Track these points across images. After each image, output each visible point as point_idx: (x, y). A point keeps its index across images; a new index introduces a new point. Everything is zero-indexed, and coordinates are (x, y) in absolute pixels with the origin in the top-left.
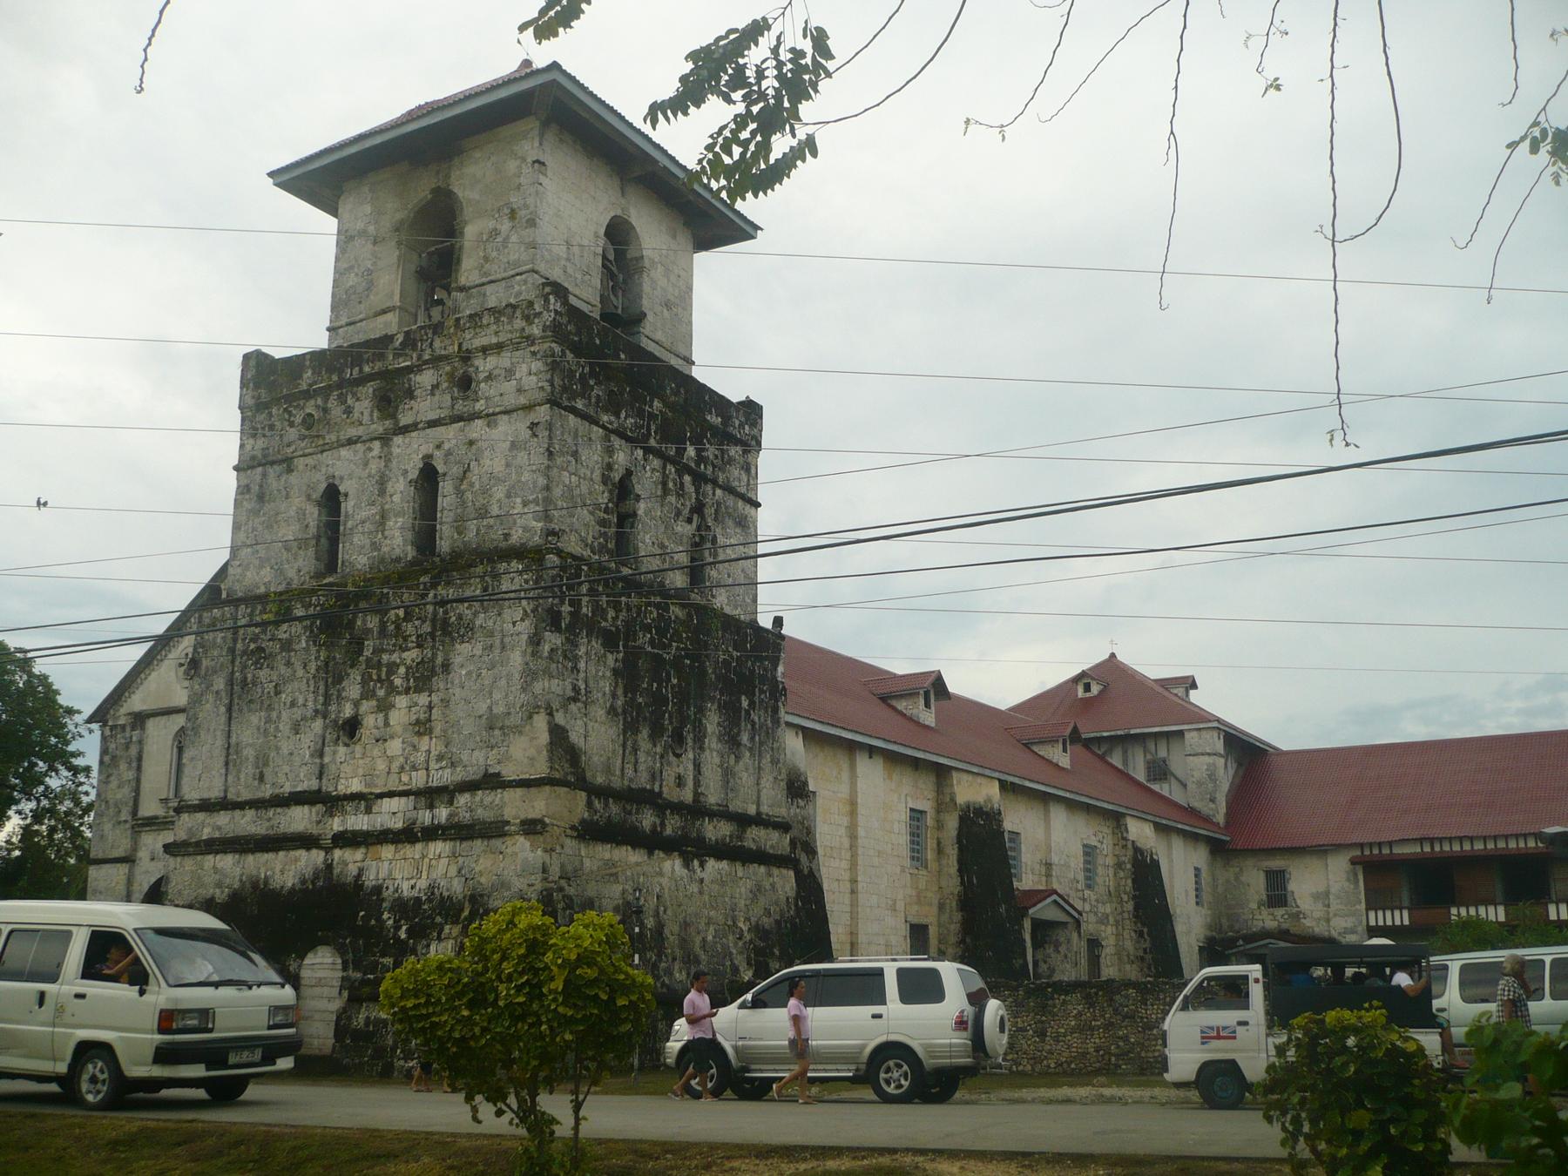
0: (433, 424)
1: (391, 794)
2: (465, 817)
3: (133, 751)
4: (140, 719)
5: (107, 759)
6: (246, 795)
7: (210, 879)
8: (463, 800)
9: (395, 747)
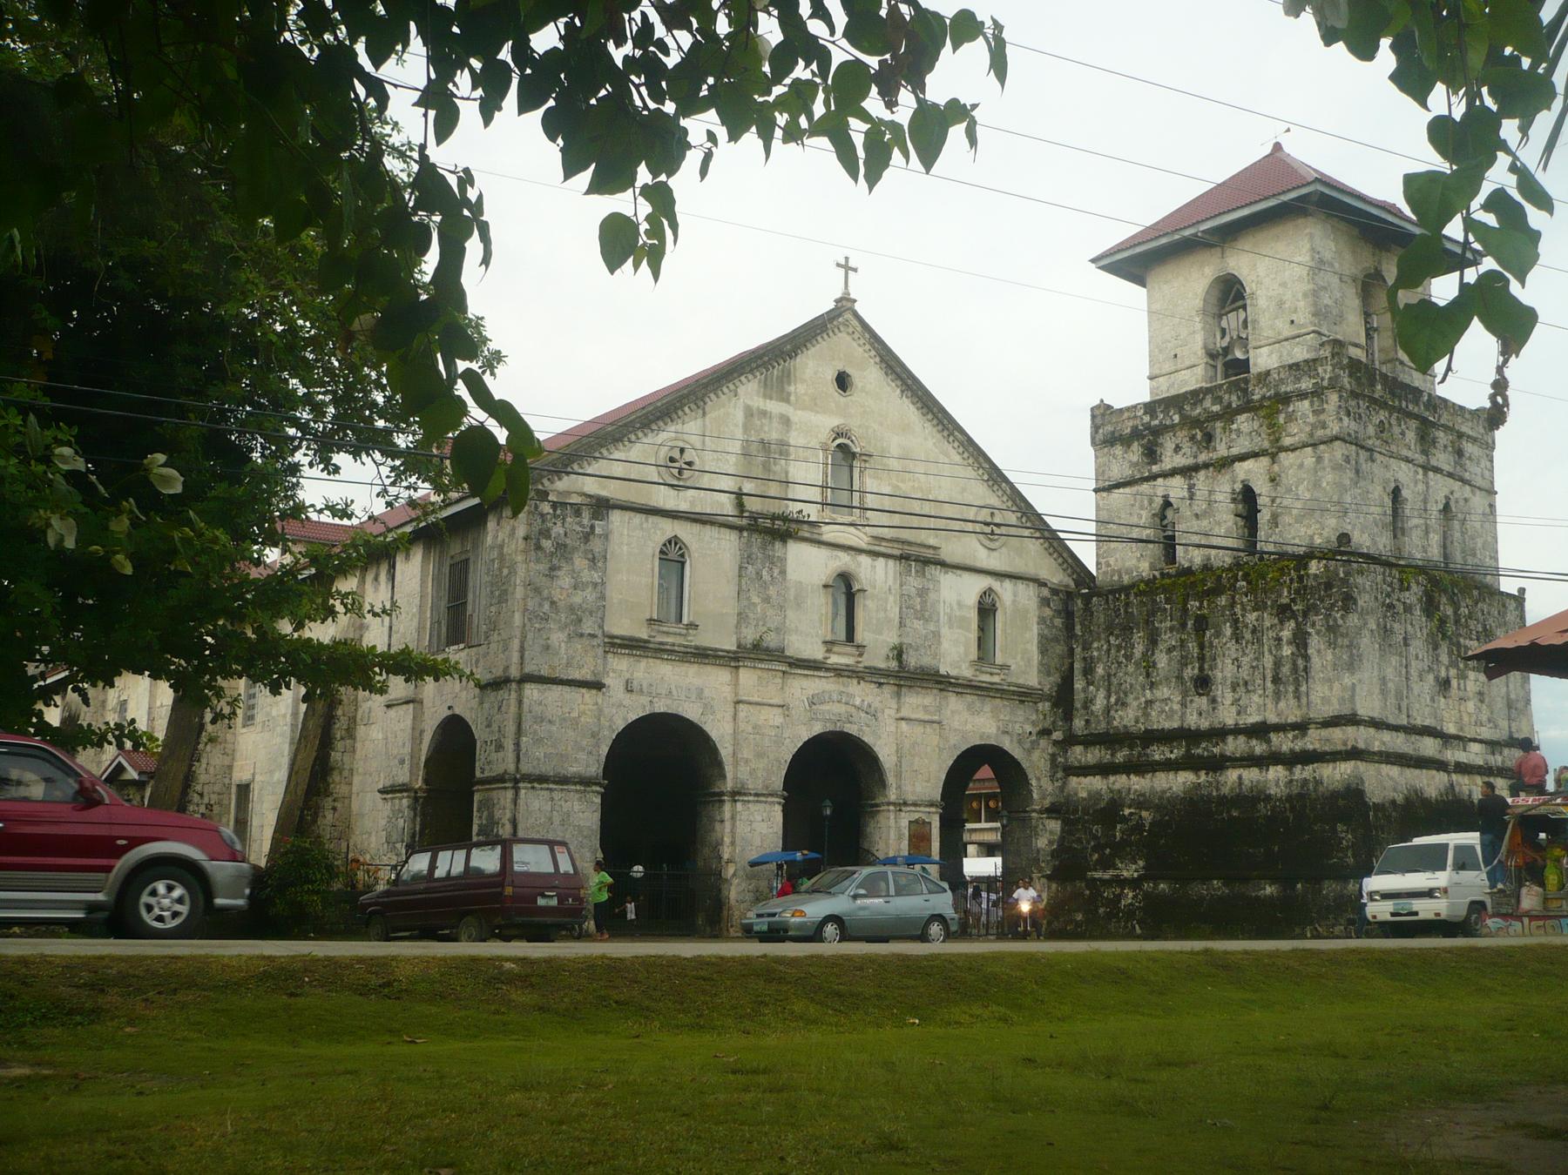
0: (1450, 475)
1: (1475, 740)
3: (596, 545)
4: (601, 506)
5: (546, 544)
6: (1392, 721)
7: (1389, 784)
8: (1506, 751)
9: (1471, 706)
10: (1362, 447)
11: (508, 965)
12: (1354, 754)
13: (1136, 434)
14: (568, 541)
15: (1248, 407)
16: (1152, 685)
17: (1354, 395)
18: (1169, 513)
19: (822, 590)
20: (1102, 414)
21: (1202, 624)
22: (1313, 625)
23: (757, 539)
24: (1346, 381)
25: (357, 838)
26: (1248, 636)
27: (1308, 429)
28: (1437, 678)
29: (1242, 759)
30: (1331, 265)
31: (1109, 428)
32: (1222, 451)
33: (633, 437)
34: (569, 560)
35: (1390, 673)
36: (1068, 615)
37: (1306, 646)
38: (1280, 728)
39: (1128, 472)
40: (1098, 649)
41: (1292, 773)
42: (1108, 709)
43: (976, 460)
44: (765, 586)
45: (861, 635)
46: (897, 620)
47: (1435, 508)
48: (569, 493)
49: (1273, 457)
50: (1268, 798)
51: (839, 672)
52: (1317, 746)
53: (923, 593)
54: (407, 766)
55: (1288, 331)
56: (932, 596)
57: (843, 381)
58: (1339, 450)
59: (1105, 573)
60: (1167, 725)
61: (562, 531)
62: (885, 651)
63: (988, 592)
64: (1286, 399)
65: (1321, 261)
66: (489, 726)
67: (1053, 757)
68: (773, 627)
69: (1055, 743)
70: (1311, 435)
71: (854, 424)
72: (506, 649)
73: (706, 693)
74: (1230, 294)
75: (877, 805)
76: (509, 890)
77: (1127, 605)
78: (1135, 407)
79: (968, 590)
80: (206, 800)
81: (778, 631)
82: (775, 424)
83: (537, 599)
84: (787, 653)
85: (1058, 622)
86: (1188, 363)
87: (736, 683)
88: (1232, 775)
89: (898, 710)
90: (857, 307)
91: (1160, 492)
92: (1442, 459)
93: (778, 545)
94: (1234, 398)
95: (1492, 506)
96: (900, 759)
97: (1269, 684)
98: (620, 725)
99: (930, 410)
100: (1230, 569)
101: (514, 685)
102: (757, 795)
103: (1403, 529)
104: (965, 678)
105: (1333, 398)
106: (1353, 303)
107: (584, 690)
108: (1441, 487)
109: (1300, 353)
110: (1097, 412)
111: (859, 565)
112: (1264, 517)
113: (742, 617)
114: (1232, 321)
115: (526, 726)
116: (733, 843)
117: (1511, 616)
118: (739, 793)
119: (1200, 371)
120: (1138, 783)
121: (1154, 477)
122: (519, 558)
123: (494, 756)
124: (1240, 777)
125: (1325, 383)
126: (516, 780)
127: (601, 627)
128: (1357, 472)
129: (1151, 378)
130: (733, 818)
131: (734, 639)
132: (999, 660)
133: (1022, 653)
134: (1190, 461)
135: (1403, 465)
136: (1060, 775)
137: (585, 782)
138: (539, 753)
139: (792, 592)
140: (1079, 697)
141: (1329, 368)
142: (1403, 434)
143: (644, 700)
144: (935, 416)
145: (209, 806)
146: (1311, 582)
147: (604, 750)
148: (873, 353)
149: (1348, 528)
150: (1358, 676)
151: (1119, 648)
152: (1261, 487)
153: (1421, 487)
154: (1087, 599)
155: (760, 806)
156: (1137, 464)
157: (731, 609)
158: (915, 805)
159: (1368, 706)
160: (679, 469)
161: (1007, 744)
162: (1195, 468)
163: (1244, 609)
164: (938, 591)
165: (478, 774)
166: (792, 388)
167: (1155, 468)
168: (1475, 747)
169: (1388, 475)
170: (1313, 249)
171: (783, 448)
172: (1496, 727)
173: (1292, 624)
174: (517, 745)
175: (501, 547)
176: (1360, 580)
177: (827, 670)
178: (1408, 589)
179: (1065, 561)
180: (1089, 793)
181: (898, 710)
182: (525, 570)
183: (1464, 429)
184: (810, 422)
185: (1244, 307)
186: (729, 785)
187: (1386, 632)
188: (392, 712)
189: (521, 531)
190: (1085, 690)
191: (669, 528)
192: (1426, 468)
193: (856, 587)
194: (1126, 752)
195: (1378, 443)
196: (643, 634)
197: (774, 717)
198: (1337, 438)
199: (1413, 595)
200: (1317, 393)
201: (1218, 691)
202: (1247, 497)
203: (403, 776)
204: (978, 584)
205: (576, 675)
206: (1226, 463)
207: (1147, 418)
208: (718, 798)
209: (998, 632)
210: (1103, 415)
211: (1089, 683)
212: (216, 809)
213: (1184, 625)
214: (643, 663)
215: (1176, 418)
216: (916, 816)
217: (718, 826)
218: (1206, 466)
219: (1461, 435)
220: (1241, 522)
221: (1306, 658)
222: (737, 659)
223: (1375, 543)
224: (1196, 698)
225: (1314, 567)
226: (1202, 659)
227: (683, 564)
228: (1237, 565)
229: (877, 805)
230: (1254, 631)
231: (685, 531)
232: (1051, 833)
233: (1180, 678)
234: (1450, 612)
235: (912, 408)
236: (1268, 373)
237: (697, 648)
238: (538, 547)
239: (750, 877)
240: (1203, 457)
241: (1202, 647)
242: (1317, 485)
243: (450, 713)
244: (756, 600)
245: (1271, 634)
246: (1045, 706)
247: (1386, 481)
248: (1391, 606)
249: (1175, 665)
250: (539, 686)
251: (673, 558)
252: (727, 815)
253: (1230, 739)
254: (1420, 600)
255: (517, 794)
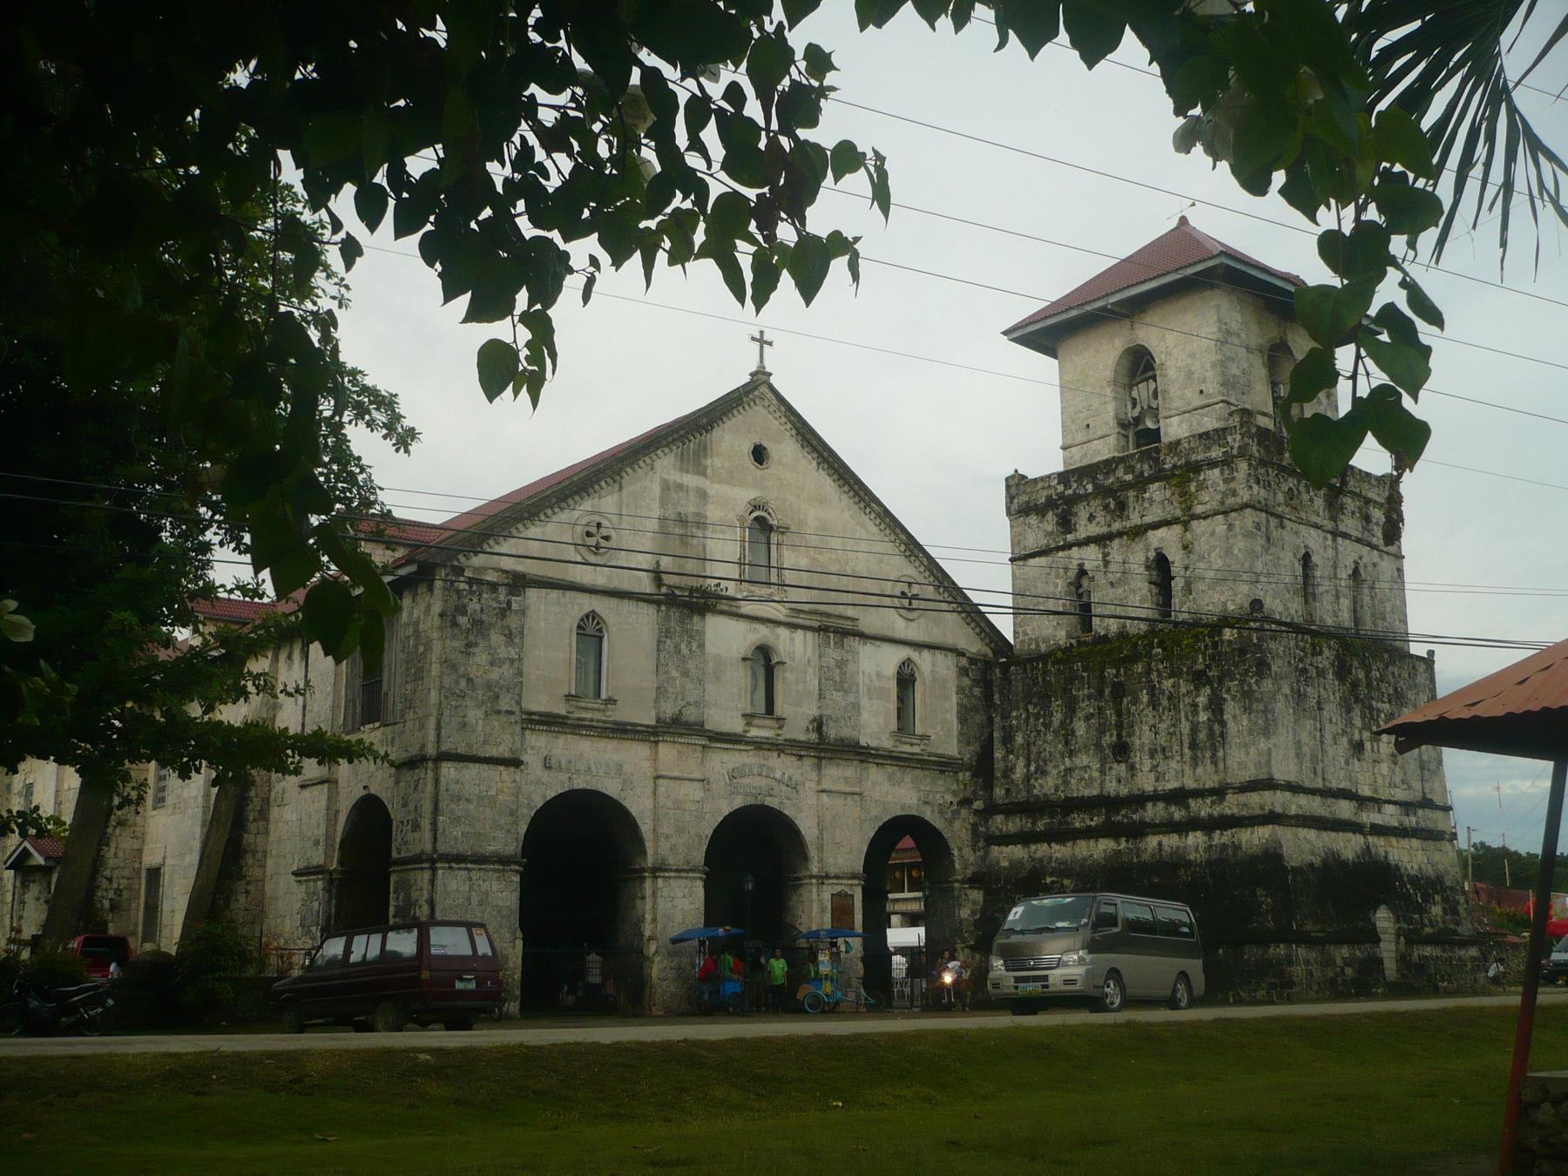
0: (1358, 541)
1: (1389, 802)
2: (1423, 825)
3: (513, 621)
4: (519, 583)
5: (463, 620)
6: (1307, 784)
7: (1307, 847)
8: (1420, 812)
9: (1385, 768)
10: (1272, 514)
11: (423, 1057)
12: (1272, 818)
13: (1051, 504)
14: (484, 617)
15: (1159, 476)
16: (1072, 754)
17: (1263, 463)
18: (1085, 582)
19: (741, 663)
20: (1016, 484)
21: (1119, 691)
22: (1228, 691)
23: (675, 614)
24: (1254, 449)
25: (271, 923)
26: (1165, 703)
27: (1219, 497)
28: (1350, 741)
29: (1161, 825)
30: (1238, 336)
31: (1024, 498)
32: (1135, 519)
33: (549, 512)
34: (485, 636)
35: (1304, 737)
36: (986, 683)
37: (1221, 712)
38: (1199, 793)
39: (1044, 542)
40: (1017, 718)
41: (1211, 838)
42: (1027, 778)
43: (893, 531)
44: (683, 660)
45: (780, 708)
46: (816, 692)
47: (1344, 574)
48: (486, 569)
49: (1186, 526)
50: (1189, 864)
51: (759, 745)
52: (1235, 811)
53: (841, 664)
54: (321, 847)
55: (1197, 401)
56: (851, 667)
57: (759, 454)
58: (1250, 517)
59: (1023, 642)
60: (1087, 793)
61: (478, 607)
62: (805, 723)
63: (907, 662)
64: (1196, 468)
65: (1228, 332)
66: (404, 805)
67: (974, 826)
68: (692, 700)
69: (976, 812)
70: (1222, 503)
71: (771, 496)
72: (422, 727)
73: (626, 768)
74: (1140, 365)
75: (799, 879)
76: (425, 975)
77: (1045, 673)
78: (1049, 477)
79: (887, 660)
80: (115, 886)
81: (697, 704)
82: (692, 498)
83: (454, 677)
84: (707, 727)
85: (977, 691)
86: (1100, 433)
87: (655, 759)
88: (1152, 842)
89: (819, 783)
90: (772, 380)
91: (1075, 562)
92: (1350, 524)
93: (696, 618)
94: (1146, 467)
95: (1400, 571)
96: (821, 831)
97: (1186, 750)
98: (539, 802)
99: (846, 482)
100: (1145, 636)
101: (430, 764)
102: (677, 871)
103: (1314, 595)
104: (884, 749)
105: (1243, 466)
106: (1260, 372)
107: (502, 768)
108: (1350, 552)
109: (1209, 423)
110: (1011, 482)
111: (778, 637)
112: (1177, 585)
113: (661, 692)
114: (1142, 391)
115: (443, 804)
116: (654, 920)
117: (1421, 679)
118: (660, 870)
119: (1112, 440)
120: (1059, 851)
121: (1068, 546)
122: (435, 635)
123: (410, 836)
124: (1160, 844)
125: (1235, 452)
126: (432, 861)
127: (518, 703)
128: (1268, 539)
129: (1064, 448)
130: (654, 894)
131: (653, 714)
132: (919, 730)
133: (941, 723)
134: (1105, 530)
135: (1312, 530)
136: (981, 844)
137: (503, 860)
138: (457, 832)
139: (711, 665)
140: (999, 766)
141: (1238, 437)
142: (1311, 500)
143: (564, 776)
144: (852, 488)
145: (119, 892)
146: (1225, 648)
147: (523, 828)
148: (789, 426)
149: (1260, 594)
150: (1273, 740)
151: (1037, 716)
152: (1175, 556)
153: (1330, 553)
154: (1005, 668)
155: (682, 882)
156: (1052, 533)
157: (650, 684)
158: (837, 877)
159: (1284, 770)
160: (596, 542)
161: (928, 815)
162: (1110, 537)
163: (1160, 675)
164: (856, 662)
165: (394, 855)
166: (708, 462)
167: (1070, 537)
168: (1390, 809)
169: (1298, 542)
170: (1220, 320)
171: (701, 524)
172: (1409, 788)
173: (1208, 690)
174: (434, 825)
175: (417, 624)
176: (1273, 645)
177: (747, 743)
178: (1321, 653)
179: (982, 630)
180: (1011, 861)
181: (819, 783)
182: (441, 647)
183: (1371, 495)
184: (727, 495)
185: (1154, 378)
186: (650, 861)
187: (1300, 697)
188: (306, 793)
189: (437, 608)
190: (1004, 759)
191: (586, 603)
192: (1335, 534)
193: (775, 660)
194: (1046, 820)
195: (1287, 510)
196: (561, 709)
197: (694, 792)
198: (1246, 506)
199: (1326, 659)
200: (1227, 462)
201: (1136, 758)
202: (1161, 566)
203: (318, 858)
204: (896, 655)
205: (494, 752)
206: (1139, 532)
207: (1061, 488)
208: (638, 875)
209: (918, 702)
210: (1018, 485)
211: (1009, 752)
212: (125, 894)
213: (1101, 692)
214: (562, 739)
215: (1090, 488)
216: (839, 889)
217: (638, 902)
218: (1120, 534)
219: (1368, 501)
220: (1155, 590)
221: (1223, 724)
222: (656, 734)
223: (1287, 609)
224: (1115, 765)
225: (1228, 634)
226: (1119, 726)
227: (601, 638)
228: (1152, 633)
229: (799, 879)
230: (1170, 698)
231: (602, 606)
232: (974, 903)
233: (1098, 745)
234: (1361, 675)
235: (829, 480)
236: (1178, 442)
237: (615, 723)
238: (455, 624)
239: (671, 955)
240: (1117, 526)
241: (1119, 714)
242: (1228, 552)
243: (365, 792)
244: (674, 674)
245: (1187, 700)
246: (965, 776)
247: (1297, 548)
248: (1304, 671)
249: (1093, 732)
250: (456, 764)
251: (590, 633)
252: (648, 892)
253: (1149, 805)
254: (1332, 665)
255: (434, 875)
